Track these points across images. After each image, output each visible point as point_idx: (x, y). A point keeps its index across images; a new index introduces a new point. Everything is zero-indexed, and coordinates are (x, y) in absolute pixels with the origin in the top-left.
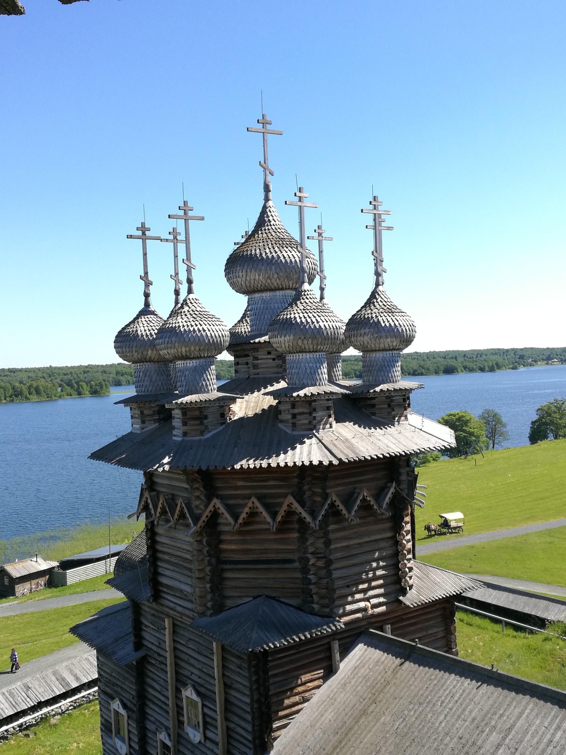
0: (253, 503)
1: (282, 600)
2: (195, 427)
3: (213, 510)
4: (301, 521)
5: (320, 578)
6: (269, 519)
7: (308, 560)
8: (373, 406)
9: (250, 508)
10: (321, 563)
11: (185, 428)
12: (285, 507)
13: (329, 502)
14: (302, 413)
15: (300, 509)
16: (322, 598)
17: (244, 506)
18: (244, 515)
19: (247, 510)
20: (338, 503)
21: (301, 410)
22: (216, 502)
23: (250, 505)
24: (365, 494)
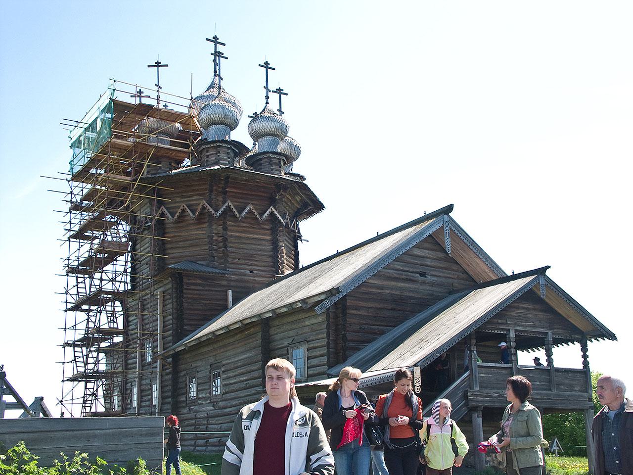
0: (183, 206)
1: (199, 262)
2: (153, 168)
3: (161, 213)
4: (210, 215)
5: (219, 248)
6: (191, 215)
7: (213, 236)
8: (261, 164)
9: (181, 210)
10: (220, 239)
11: (148, 169)
12: (200, 207)
13: (227, 205)
14: (212, 154)
15: (209, 207)
16: (220, 258)
17: (179, 207)
18: (178, 214)
19: (180, 211)
20: (232, 207)
21: (211, 153)
22: (163, 207)
23: (182, 208)
24: (251, 208)
